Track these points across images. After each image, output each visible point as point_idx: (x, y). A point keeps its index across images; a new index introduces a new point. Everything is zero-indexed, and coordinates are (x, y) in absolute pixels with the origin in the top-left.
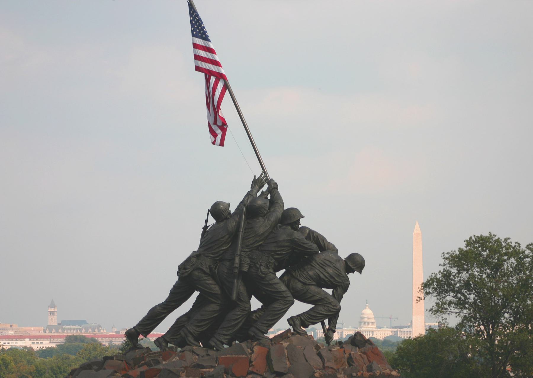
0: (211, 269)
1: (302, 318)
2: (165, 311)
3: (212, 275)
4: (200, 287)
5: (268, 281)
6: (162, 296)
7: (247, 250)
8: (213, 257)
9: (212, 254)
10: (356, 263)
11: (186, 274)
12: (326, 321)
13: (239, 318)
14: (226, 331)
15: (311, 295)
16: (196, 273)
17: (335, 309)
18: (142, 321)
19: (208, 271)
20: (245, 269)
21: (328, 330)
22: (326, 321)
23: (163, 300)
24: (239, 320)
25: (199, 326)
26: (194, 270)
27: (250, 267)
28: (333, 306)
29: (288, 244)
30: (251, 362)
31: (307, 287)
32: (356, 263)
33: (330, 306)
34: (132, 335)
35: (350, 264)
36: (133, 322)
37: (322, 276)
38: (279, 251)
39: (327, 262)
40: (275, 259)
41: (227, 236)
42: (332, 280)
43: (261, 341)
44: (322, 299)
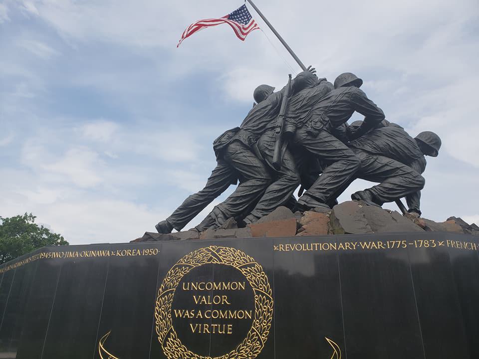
0: (250, 140)
1: (372, 191)
2: (201, 199)
3: (250, 148)
4: (237, 161)
5: (321, 139)
6: (198, 184)
7: (293, 116)
8: (253, 130)
9: (254, 127)
10: (430, 145)
11: (221, 146)
12: (403, 200)
13: (284, 189)
14: (266, 206)
15: (380, 165)
16: (232, 146)
17: (418, 181)
18: (176, 211)
19: (247, 143)
20: (290, 129)
21: (409, 211)
22: (403, 200)
23: (201, 190)
24: (285, 191)
25: (234, 206)
26: (231, 143)
27: (297, 128)
28: (415, 177)
29: (345, 98)
30: (299, 226)
31: (375, 157)
32: (430, 145)
33: (411, 177)
34: (164, 228)
35: (423, 140)
36: (165, 214)
37: (392, 145)
38: (334, 106)
39: (394, 133)
40: (328, 117)
41: (271, 106)
42: (406, 151)
43: (315, 209)
44: (398, 168)
